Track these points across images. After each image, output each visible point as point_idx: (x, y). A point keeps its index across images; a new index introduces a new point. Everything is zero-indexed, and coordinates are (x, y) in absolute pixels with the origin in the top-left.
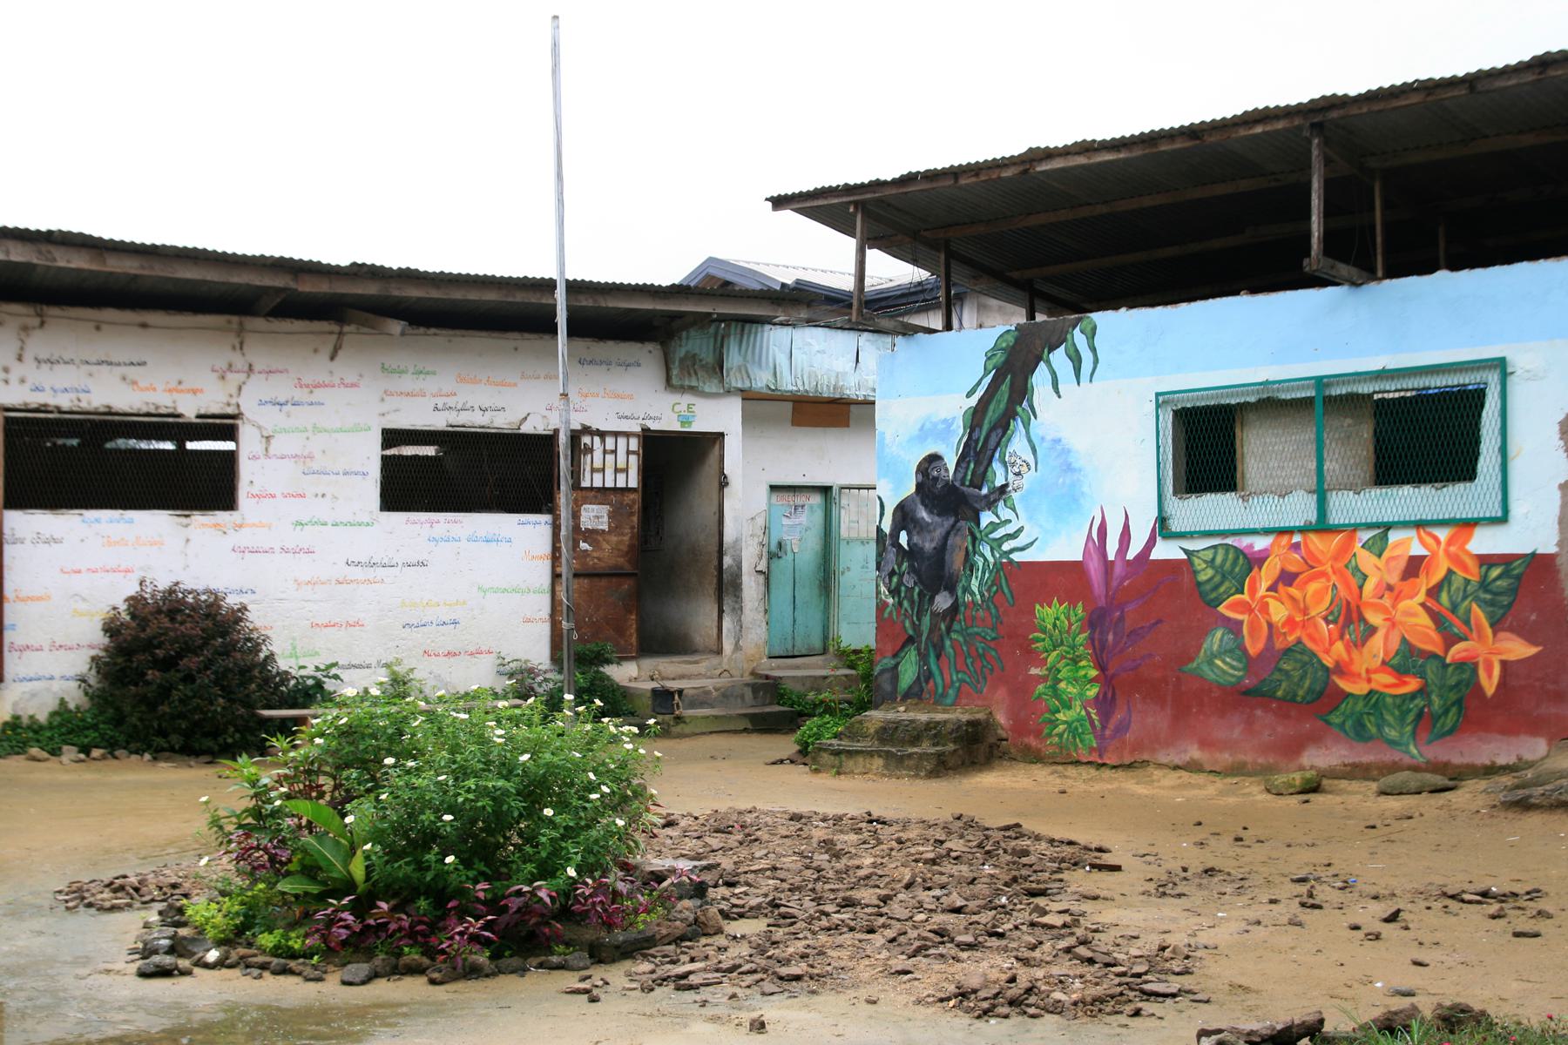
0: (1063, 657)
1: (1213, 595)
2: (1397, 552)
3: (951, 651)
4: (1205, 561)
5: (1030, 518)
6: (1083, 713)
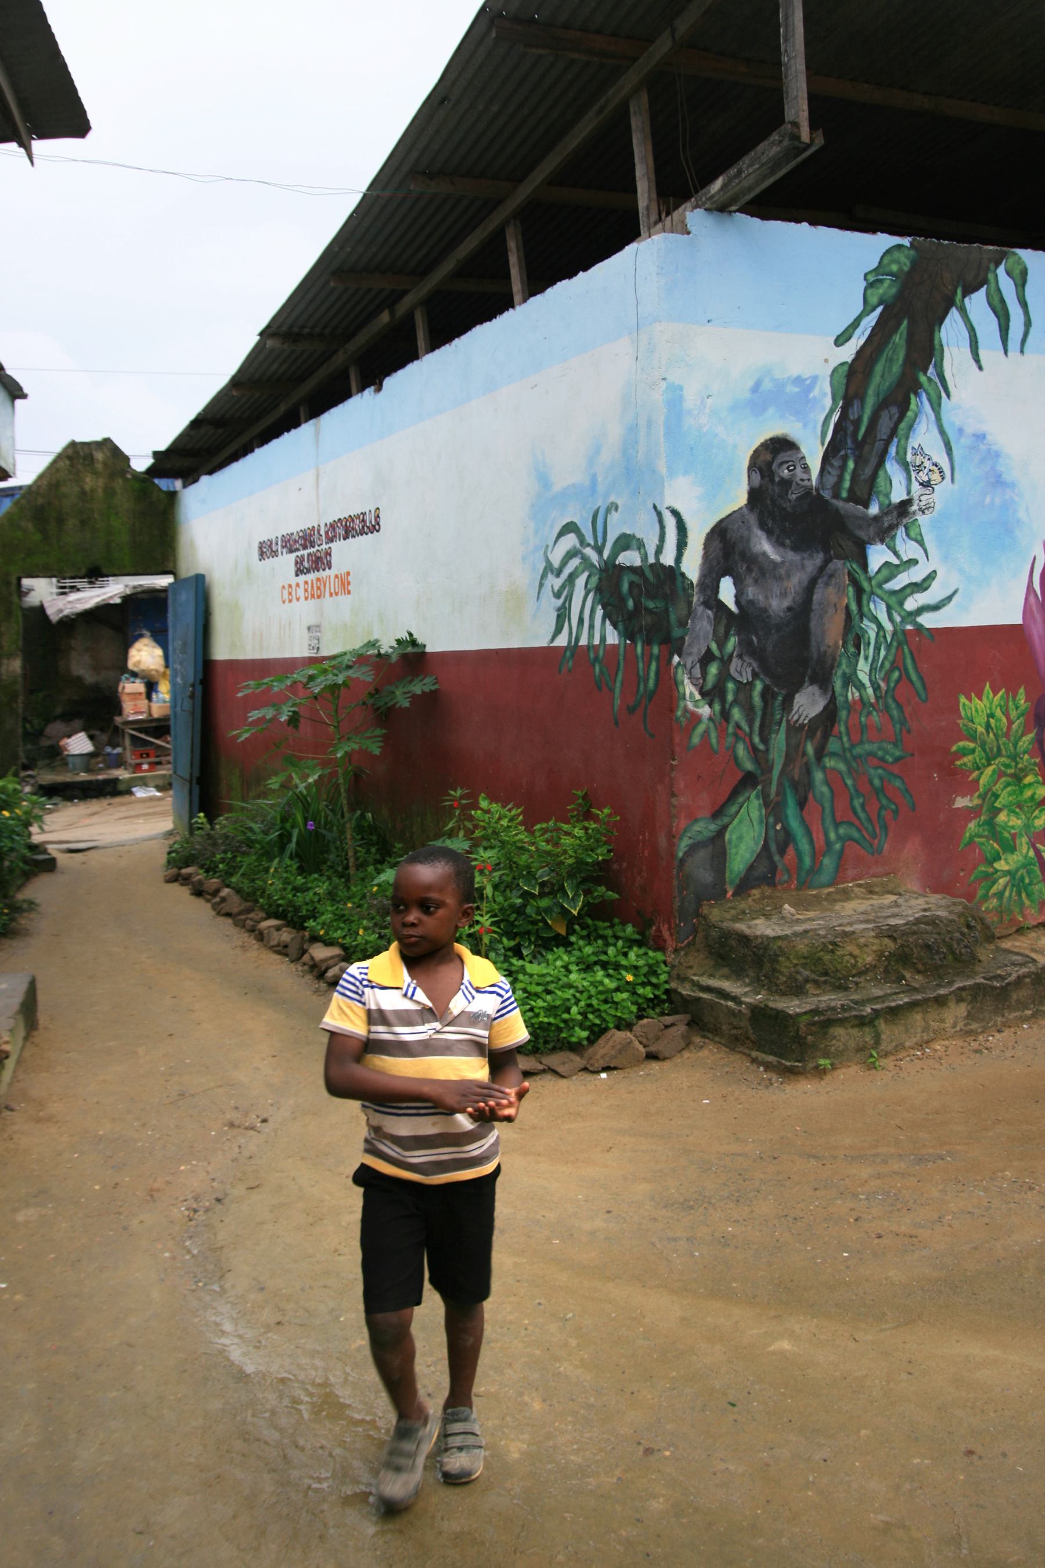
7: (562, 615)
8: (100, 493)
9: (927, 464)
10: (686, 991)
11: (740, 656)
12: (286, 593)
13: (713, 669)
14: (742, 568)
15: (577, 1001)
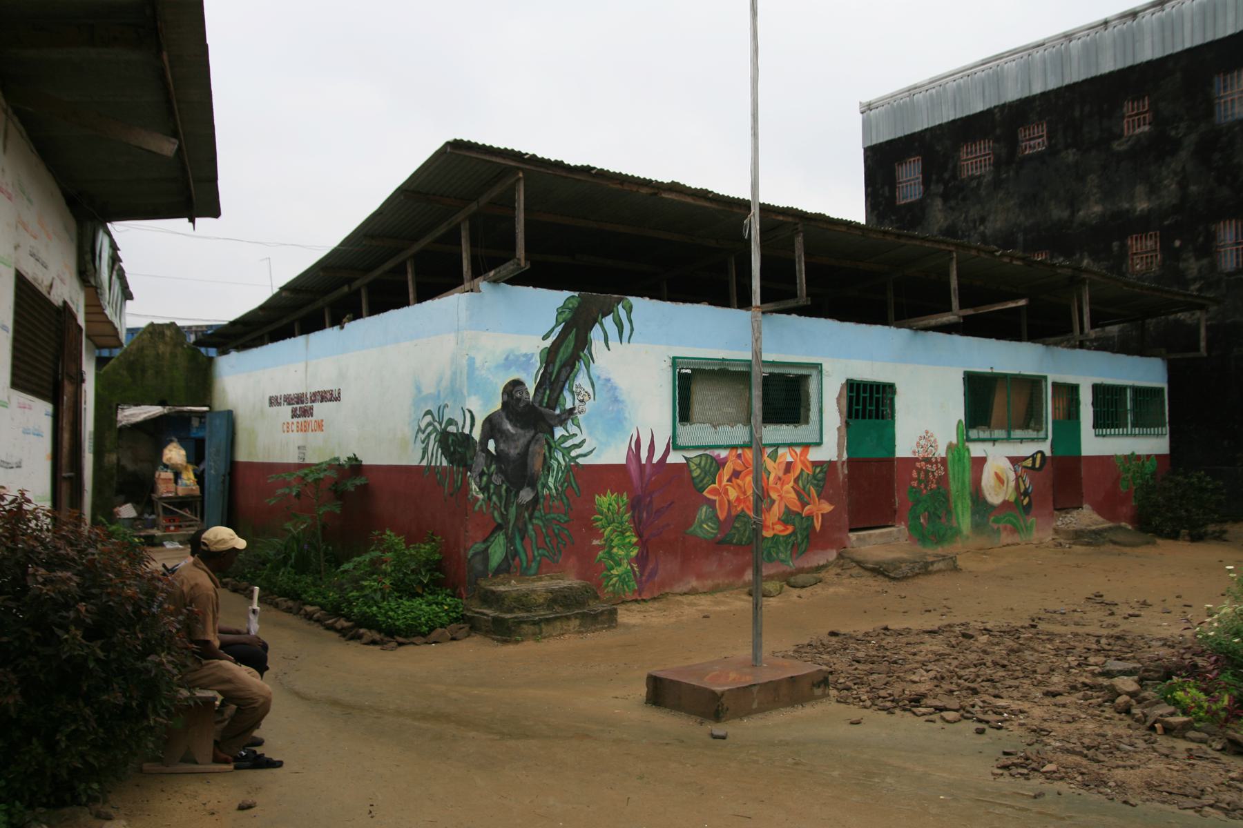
0: (615, 531)
1: (701, 485)
2: (781, 460)
3: (533, 533)
4: (696, 465)
5: (590, 434)
6: (629, 567)
7: (425, 451)
8: (168, 355)
9: (582, 392)
10: (469, 614)
11: (496, 473)
12: (285, 427)
13: (485, 479)
14: (498, 436)
15: (424, 616)
